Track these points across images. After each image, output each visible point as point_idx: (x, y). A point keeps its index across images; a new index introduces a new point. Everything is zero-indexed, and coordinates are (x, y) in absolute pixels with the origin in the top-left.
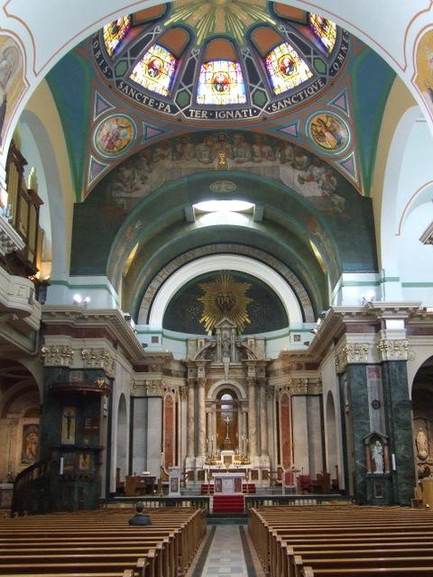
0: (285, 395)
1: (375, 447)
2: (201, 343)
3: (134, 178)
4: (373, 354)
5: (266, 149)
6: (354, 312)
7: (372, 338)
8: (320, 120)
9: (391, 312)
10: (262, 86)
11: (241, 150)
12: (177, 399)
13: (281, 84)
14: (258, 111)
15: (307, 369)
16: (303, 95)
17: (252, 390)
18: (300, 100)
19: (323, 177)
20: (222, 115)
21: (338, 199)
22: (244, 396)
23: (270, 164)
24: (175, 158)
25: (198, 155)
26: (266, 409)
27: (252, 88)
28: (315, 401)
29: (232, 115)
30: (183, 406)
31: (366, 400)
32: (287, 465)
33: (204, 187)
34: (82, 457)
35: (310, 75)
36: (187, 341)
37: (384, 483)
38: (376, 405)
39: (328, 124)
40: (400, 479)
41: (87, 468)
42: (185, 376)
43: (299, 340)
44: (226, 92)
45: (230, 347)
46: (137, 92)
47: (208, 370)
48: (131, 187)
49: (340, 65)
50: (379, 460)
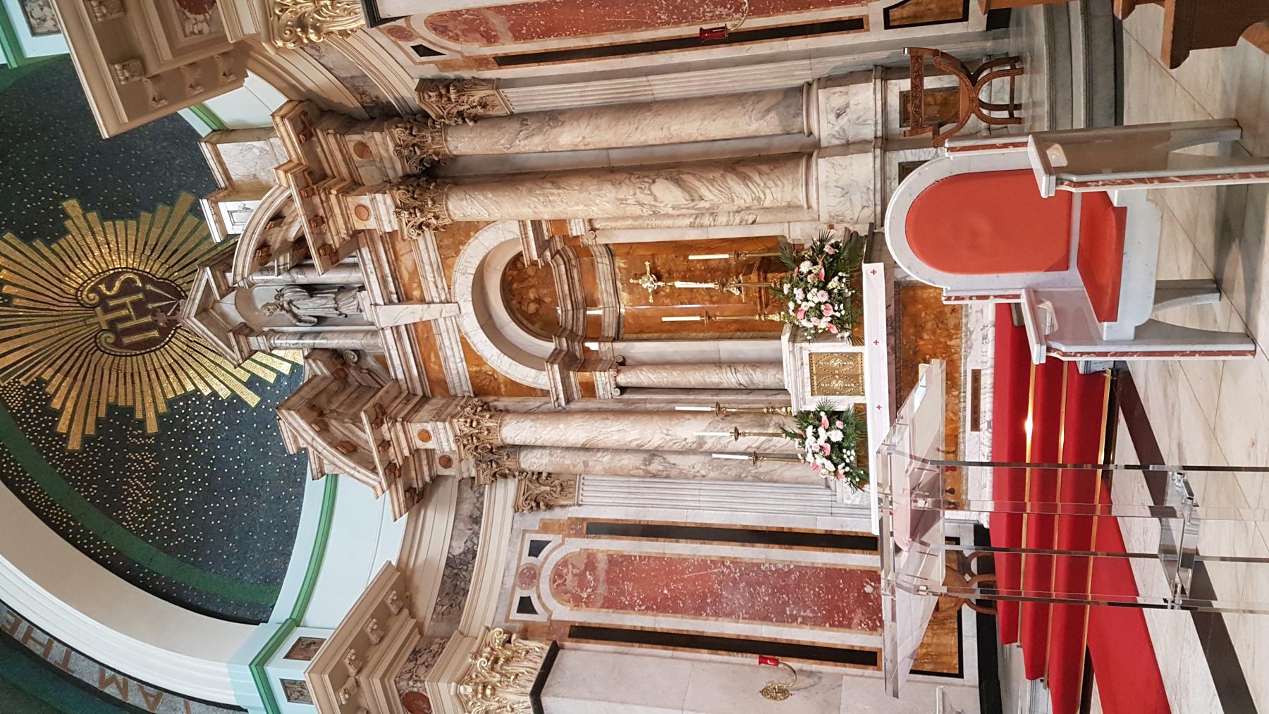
17: (461, 207)
26: (553, 117)
30: (601, 502)
45: (312, 290)
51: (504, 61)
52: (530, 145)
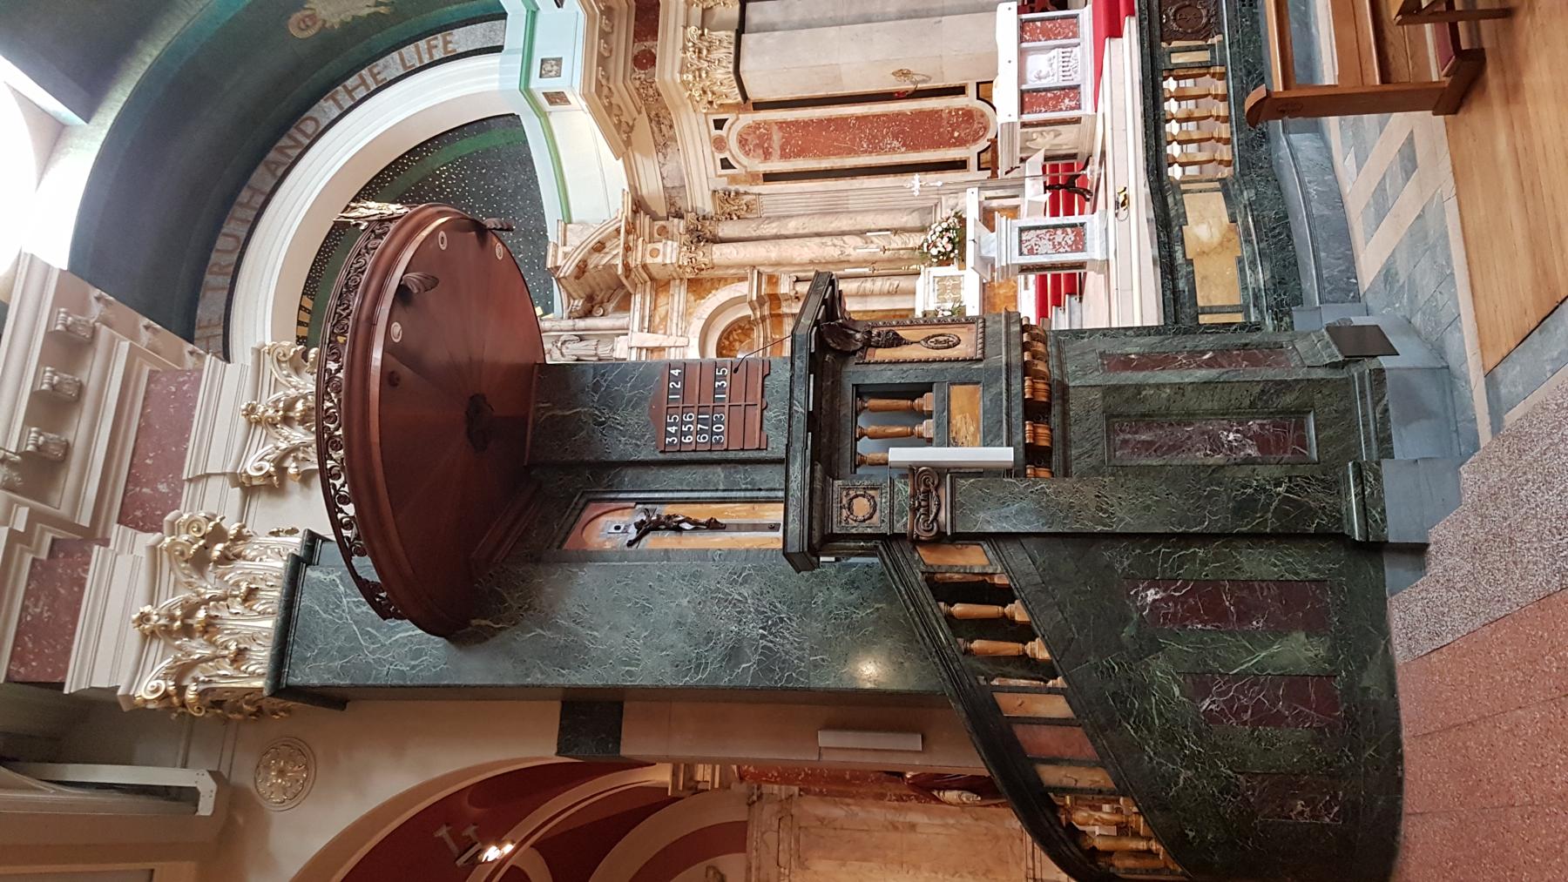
0: (743, 142)
15: (653, 33)
17: (722, 254)
22: (742, 289)
43: (559, 61)
51: (769, 177)
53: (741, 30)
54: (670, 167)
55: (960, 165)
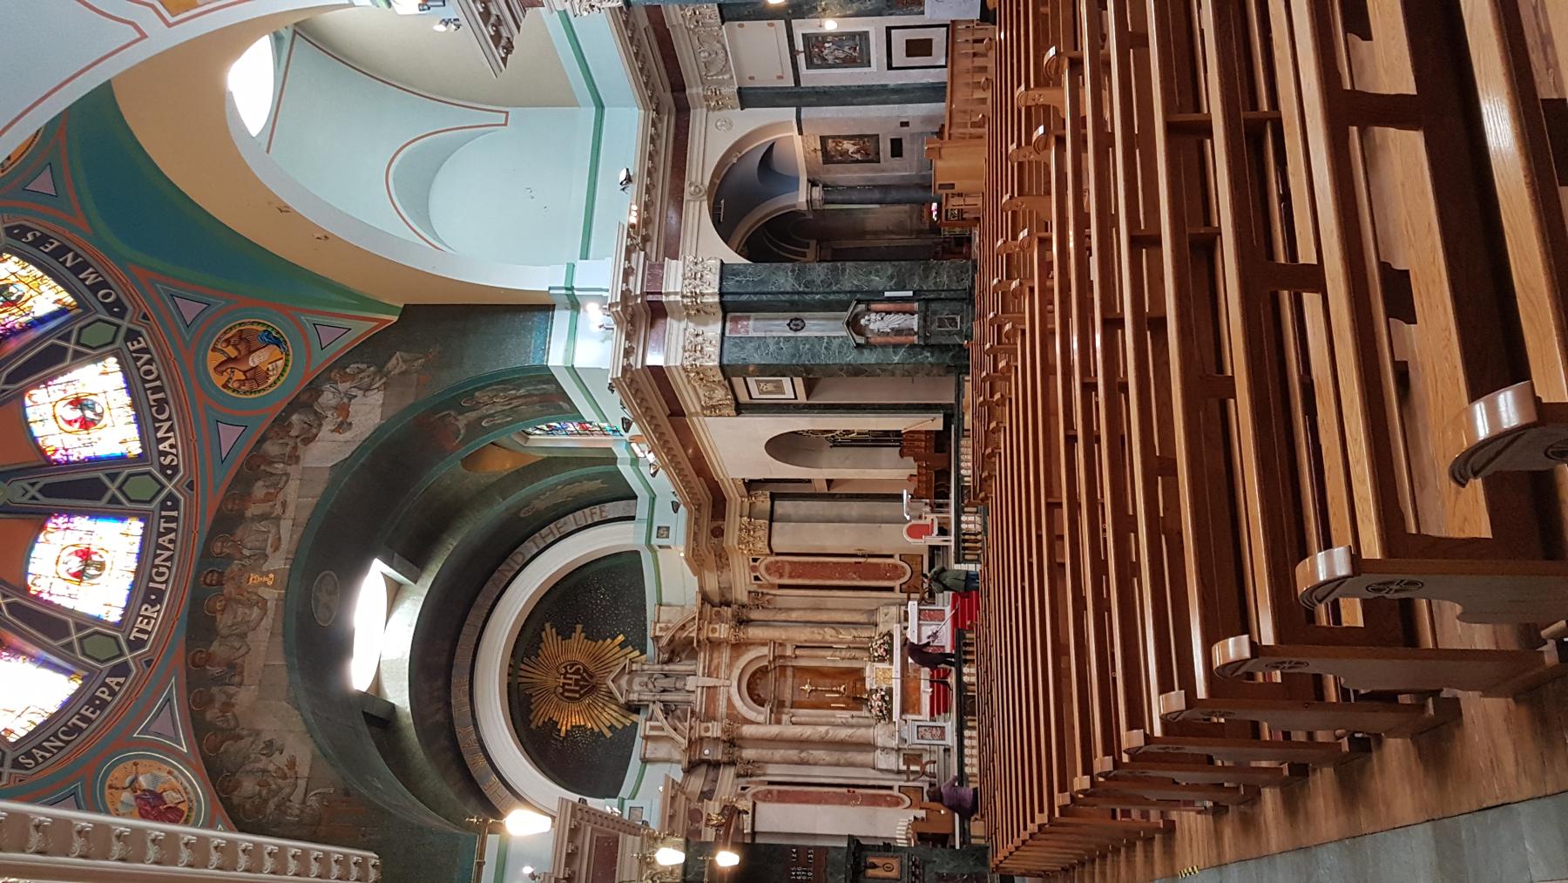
0: (767, 569)
1: (872, 326)
2: (652, 728)
3: (264, 771)
4: (706, 324)
5: (259, 490)
6: (624, 344)
7: (675, 323)
8: (219, 368)
9: (632, 279)
10: (113, 477)
11: (251, 541)
12: (762, 783)
13: (117, 435)
14: (170, 496)
16: (156, 390)
17: (754, 633)
18: (165, 401)
19: (343, 387)
20: (162, 574)
21: (396, 363)
22: (765, 650)
23: (293, 485)
24: (237, 679)
25: (244, 628)
26: (792, 609)
27: (114, 500)
28: (783, 507)
29: (168, 553)
30: (775, 772)
31: (787, 339)
32: (895, 572)
33: (322, 645)
34: (870, 872)
35: (112, 362)
36: (645, 761)
37: (935, 313)
38: (797, 325)
39: (232, 353)
40: (929, 284)
41: (895, 863)
42: (715, 765)
44: (107, 558)
46: (55, 735)
47: (710, 717)
48: (285, 777)
49: (104, 284)
50: (895, 321)
51: (781, 587)
52: (783, 616)
53: (771, 520)
54: (724, 577)
55: (891, 589)
